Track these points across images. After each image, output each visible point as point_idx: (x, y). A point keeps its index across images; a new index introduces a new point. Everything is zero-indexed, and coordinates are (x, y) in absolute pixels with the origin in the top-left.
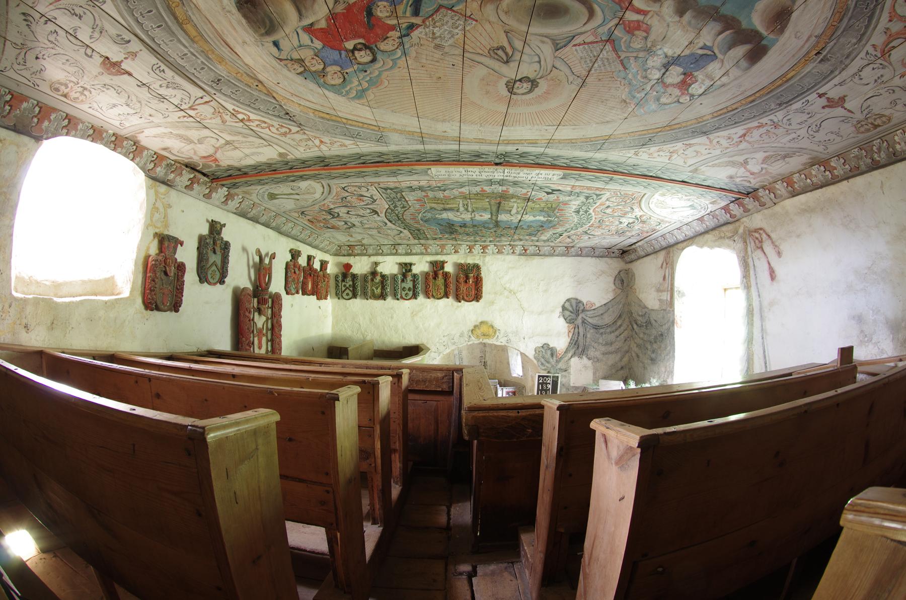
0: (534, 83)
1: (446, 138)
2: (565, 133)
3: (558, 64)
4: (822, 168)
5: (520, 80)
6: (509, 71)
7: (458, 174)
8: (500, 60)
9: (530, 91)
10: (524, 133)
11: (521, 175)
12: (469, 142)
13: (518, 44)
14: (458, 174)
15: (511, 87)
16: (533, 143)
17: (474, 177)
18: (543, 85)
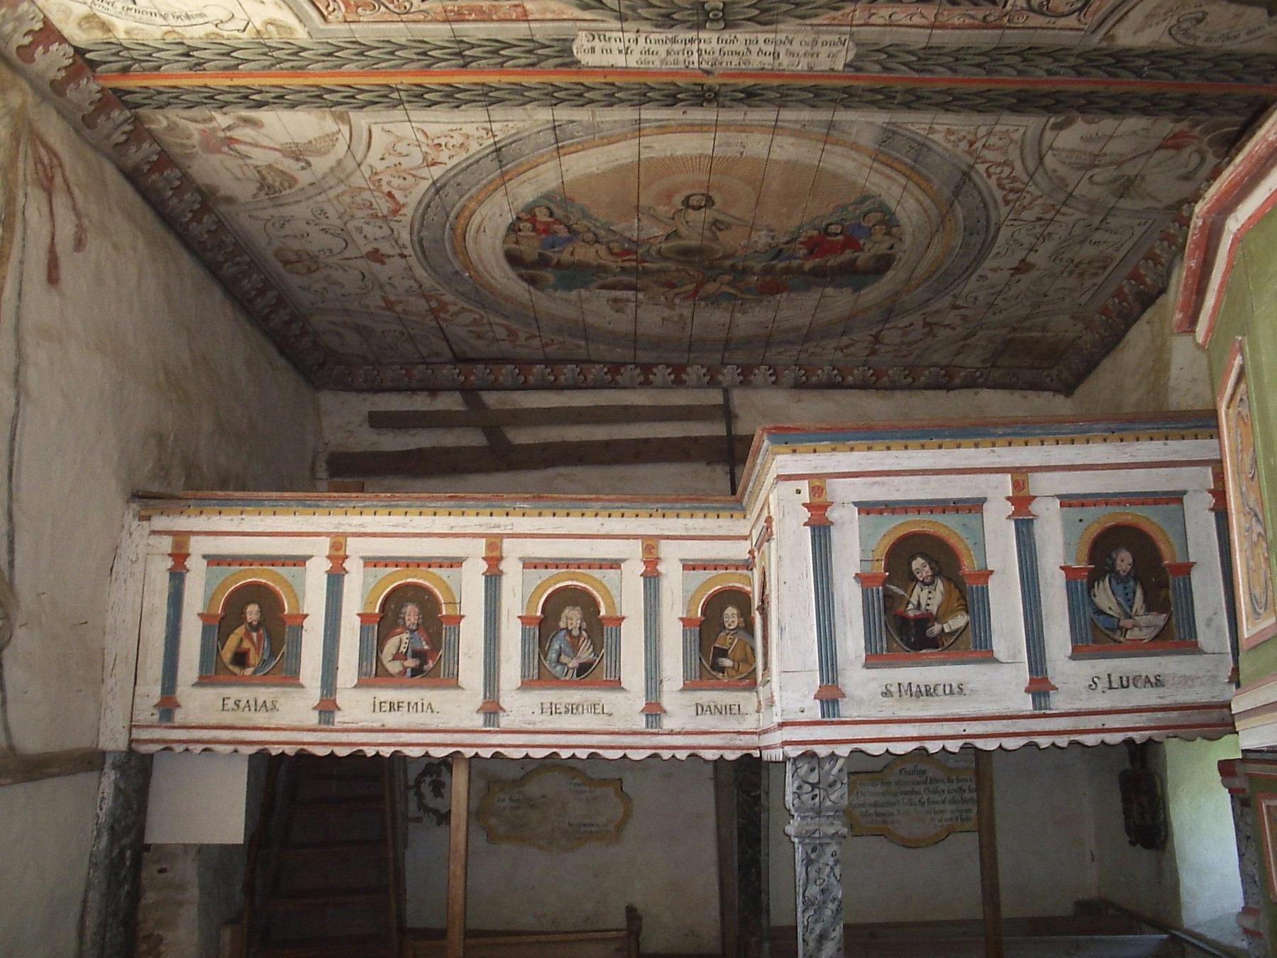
0: (686, 202)
1: (795, 134)
2: (624, 152)
3: (671, 222)
4: (197, 206)
5: (700, 207)
6: (710, 214)
7: (796, 47)
8: (722, 222)
9: (688, 198)
10: (683, 142)
11: (662, 49)
12: (762, 127)
13: (708, 234)
14: (796, 47)
15: (709, 201)
16: (663, 129)
17: (761, 37)
18: (678, 199)
